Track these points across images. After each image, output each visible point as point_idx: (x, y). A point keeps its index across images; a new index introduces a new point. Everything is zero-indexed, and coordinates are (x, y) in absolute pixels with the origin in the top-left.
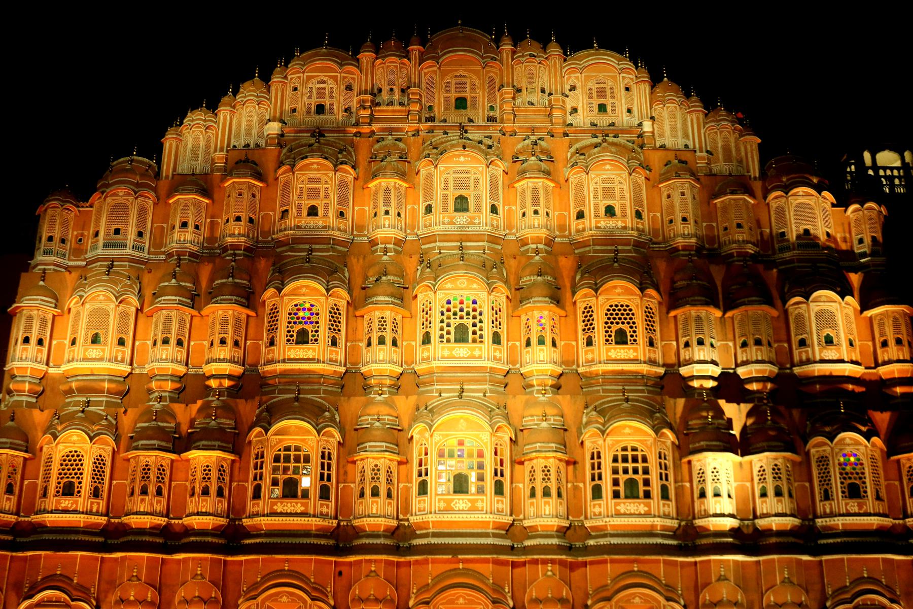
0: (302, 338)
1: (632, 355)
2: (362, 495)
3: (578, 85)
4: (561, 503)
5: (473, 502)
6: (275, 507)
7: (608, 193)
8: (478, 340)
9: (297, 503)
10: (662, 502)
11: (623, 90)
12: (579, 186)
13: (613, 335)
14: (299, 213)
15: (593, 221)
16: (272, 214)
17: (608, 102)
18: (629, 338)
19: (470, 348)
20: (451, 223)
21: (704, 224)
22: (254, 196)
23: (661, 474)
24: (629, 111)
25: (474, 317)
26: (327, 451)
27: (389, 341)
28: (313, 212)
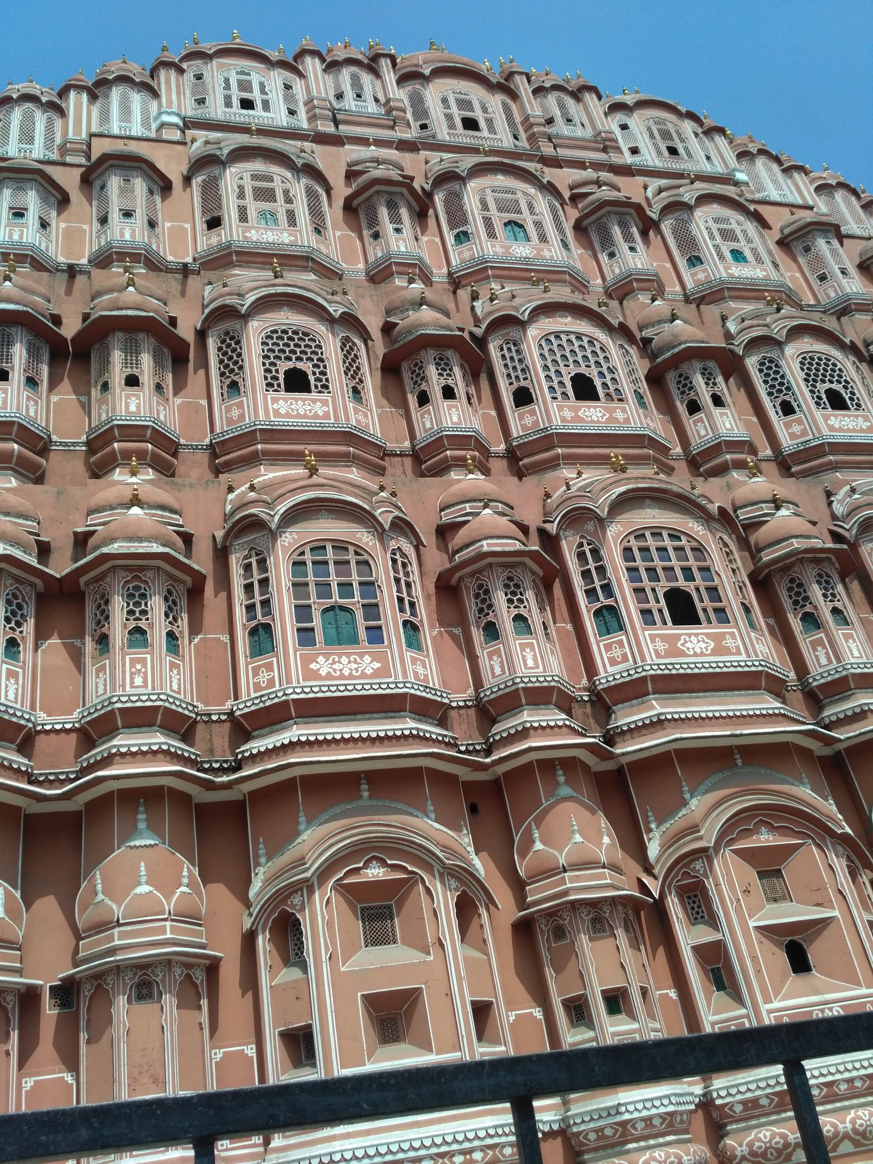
5: (718, 638)
6: (313, 666)
8: (614, 396)
9: (361, 655)
15: (721, 267)
18: (849, 402)
22: (151, 192)
24: (708, 158)
25: (598, 363)
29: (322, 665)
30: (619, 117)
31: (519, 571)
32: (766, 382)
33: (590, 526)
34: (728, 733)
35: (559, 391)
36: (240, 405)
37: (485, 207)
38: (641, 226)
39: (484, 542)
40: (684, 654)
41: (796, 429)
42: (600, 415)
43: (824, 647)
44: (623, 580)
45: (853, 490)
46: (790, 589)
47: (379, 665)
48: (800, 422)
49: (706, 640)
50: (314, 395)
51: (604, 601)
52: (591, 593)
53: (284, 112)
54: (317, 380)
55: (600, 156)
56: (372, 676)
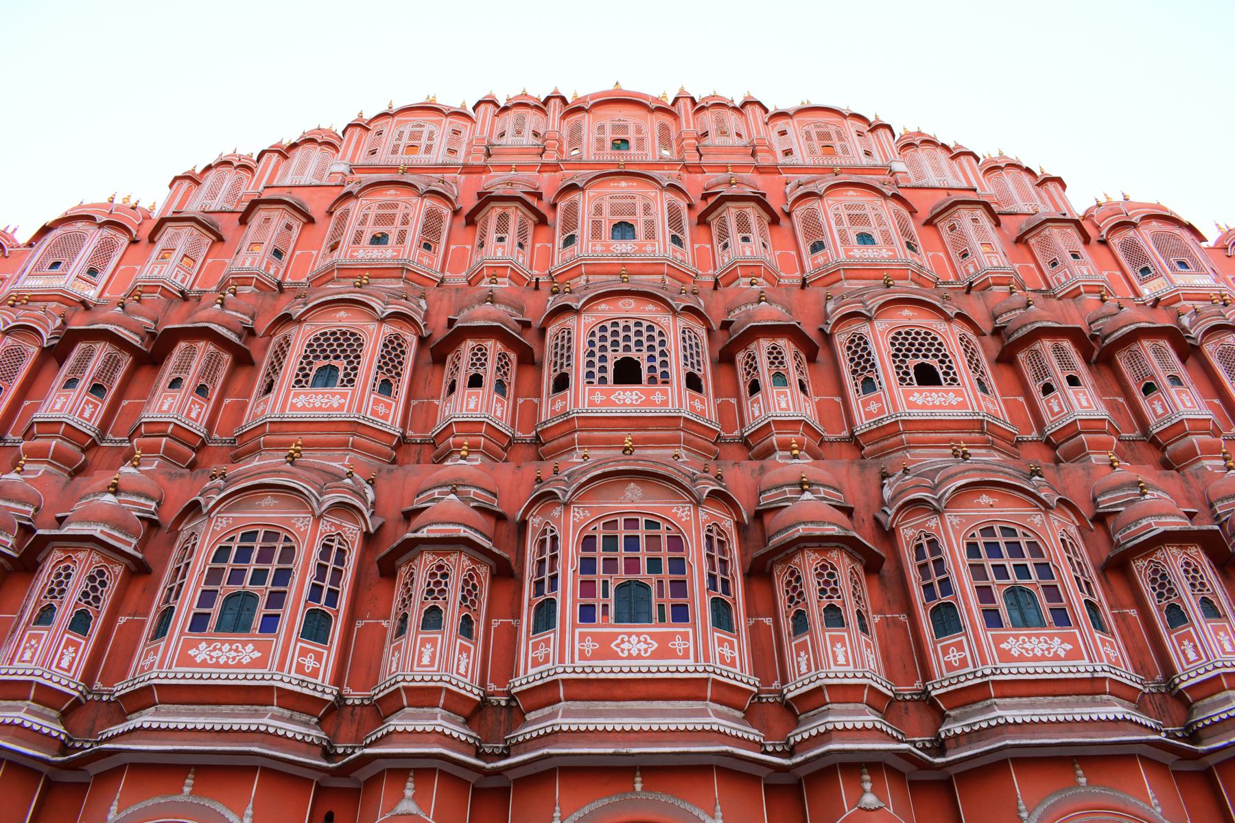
0: (327, 376)
1: (953, 399)
3: (790, 130)
4: (868, 645)
5: (663, 639)
6: (192, 652)
8: (659, 379)
9: (244, 644)
10: (1097, 635)
11: (855, 135)
13: (912, 372)
14: (357, 240)
16: (315, 253)
17: (837, 145)
18: (942, 377)
19: (642, 391)
21: (1017, 266)
22: (289, 227)
23: (1077, 578)
24: (868, 153)
25: (651, 348)
26: (335, 546)
27: (489, 379)
28: (379, 240)
29: (201, 652)
30: (781, 124)
31: (452, 559)
32: (852, 360)
33: (557, 512)
34: (611, 751)
35: (598, 375)
36: (266, 402)
37: (599, 210)
38: (766, 218)
39: (425, 530)
40: (615, 656)
41: (874, 407)
42: (635, 397)
43: (807, 652)
44: (570, 572)
46: (789, 583)
47: (259, 654)
48: (878, 400)
49: (649, 640)
50: (337, 389)
51: (548, 594)
52: (539, 584)
55: (750, 160)
56: (248, 666)
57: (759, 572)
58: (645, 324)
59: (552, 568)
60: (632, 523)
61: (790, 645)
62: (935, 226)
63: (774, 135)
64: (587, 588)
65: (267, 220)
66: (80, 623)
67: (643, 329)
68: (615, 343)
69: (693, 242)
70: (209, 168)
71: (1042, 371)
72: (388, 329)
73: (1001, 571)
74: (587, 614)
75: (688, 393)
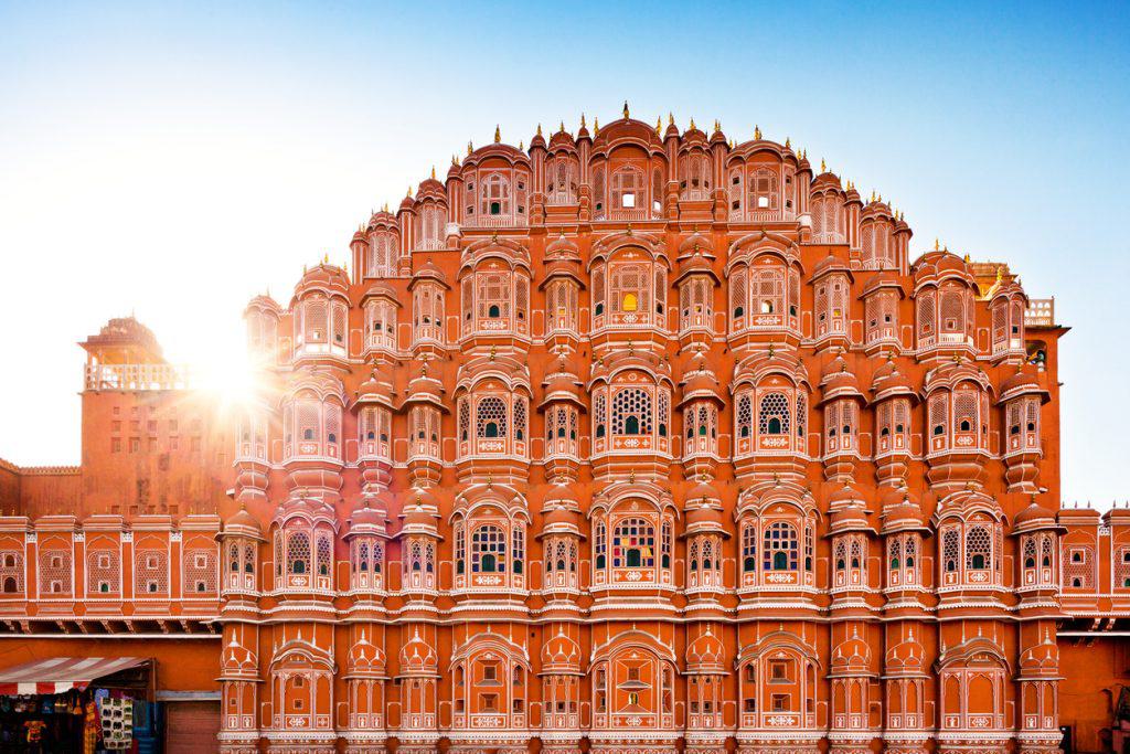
0: (491, 431)
1: (783, 442)
2: (549, 568)
5: (644, 573)
7: (766, 288)
10: (806, 573)
12: (740, 283)
15: (751, 317)
20: (621, 322)
22: (439, 298)
24: (789, 204)
25: (644, 409)
26: (518, 531)
28: (494, 312)
30: (736, 171)
33: (604, 516)
37: (616, 285)
38: (713, 283)
40: (626, 580)
45: (750, 492)
48: (747, 441)
51: (601, 553)
52: (598, 548)
53: (516, 210)
54: (501, 429)
57: (682, 540)
58: (642, 391)
59: (603, 541)
60: (634, 522)
61: (690, 573)
62: (813, 285)
63: (730, 181)
64: (617, 552)
65: (427, 295)
66: (429, 568)
67: (640, 395)
68: (626, 406)
69: (669, 305)
70: (370, 228)
71: (834, 420)
72: (515, 396)
73: (776, 545)
74: (617, 563)
75: (658, 441)
